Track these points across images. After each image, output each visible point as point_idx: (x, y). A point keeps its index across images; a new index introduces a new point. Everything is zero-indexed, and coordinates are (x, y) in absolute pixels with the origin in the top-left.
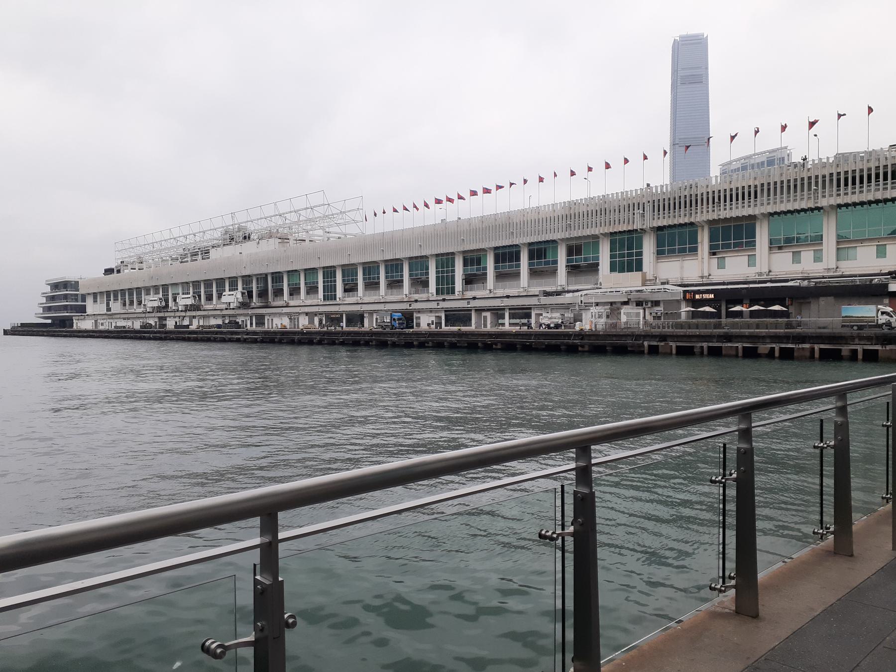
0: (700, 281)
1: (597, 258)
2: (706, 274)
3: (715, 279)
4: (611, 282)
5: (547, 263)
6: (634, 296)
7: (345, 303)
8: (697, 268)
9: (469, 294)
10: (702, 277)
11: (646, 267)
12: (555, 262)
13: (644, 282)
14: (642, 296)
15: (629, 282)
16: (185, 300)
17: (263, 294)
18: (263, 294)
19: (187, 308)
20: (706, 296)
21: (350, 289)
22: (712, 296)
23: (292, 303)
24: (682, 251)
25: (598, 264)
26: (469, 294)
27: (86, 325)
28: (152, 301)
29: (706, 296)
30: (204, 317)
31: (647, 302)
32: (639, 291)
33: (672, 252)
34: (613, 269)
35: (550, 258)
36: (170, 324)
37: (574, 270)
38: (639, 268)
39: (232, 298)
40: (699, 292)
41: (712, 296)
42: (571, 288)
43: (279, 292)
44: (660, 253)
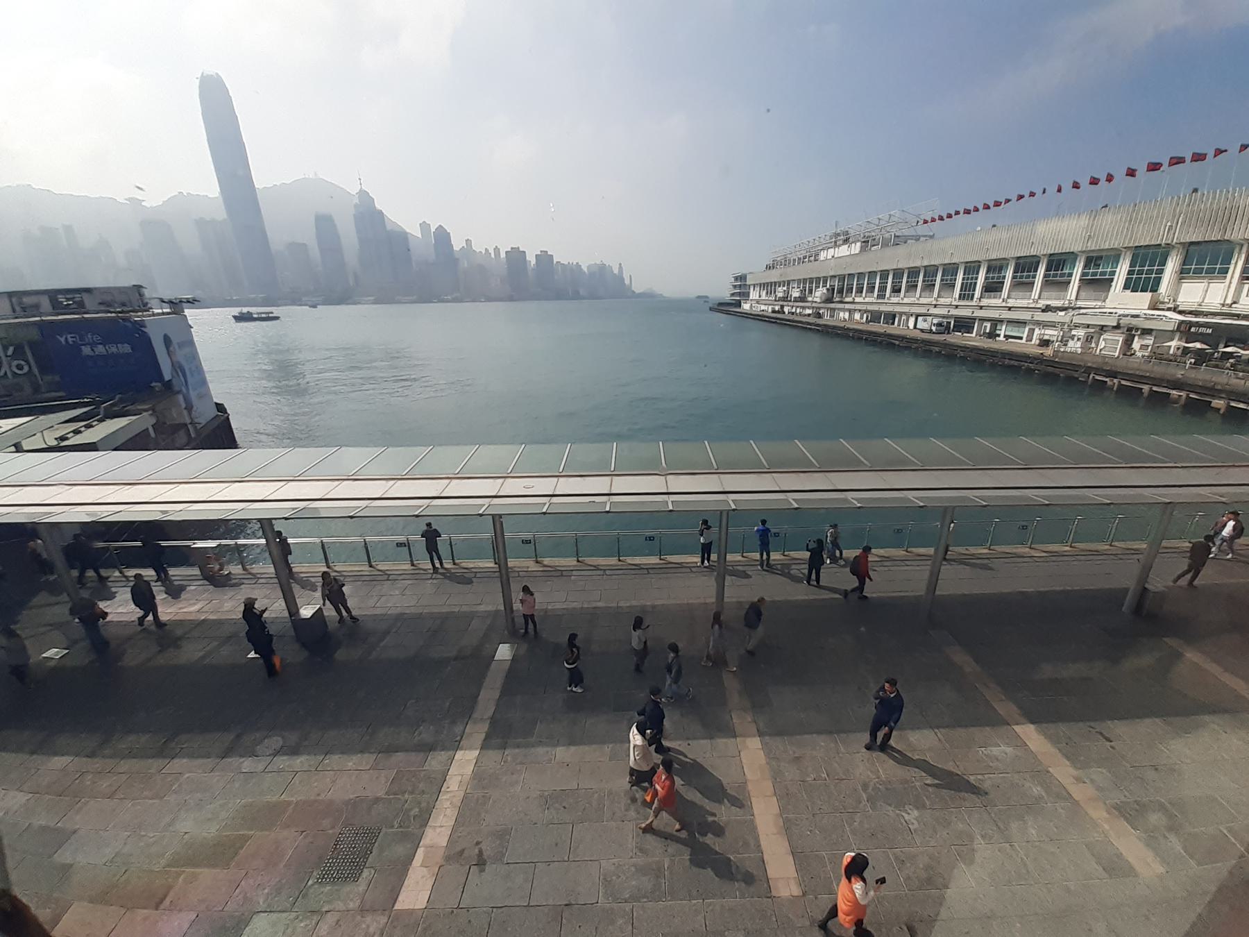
0: (1216, 308)
1: (1113, 273)
2: (1229, 301)
3: (1237, 309)
4: (1123, 302)
5: (1062, 275)
6: (1124, 321)
7: (892, 303)
8: (1207, 295)
9: (985, 302)
10: (1223, 305)
11: (1163, 288)
12: (1070, 275)
13: (1153, 307)
14: (1134, 322)
15: (1138, 303)
16: (796, 293)
17: (841, 291)
18: (841, 291)
19: (796, 300)
20: (1202, 330)
21: (896, 290)
22: (1209, 331)
23: (857, 300)
24: (1210, 271)
25: (1112, 280)
26: (985, 302)
27: (746, 307)
28: (780, 292)
29: (1202, 330)
30: (804, 308)
31: (1137, 329)
32: (1133, 316)
33: (1198, 272)
34: (1126, 287)
35: (1066, 271)
36: (786, 309)
37: (1086, 282)
38: (1154, 289)
39: (819, 293)
40: (1198, 325)
41: (1209, 331)
42: (1079, 303)
43: (850, 290)
44: (1183, 274)
